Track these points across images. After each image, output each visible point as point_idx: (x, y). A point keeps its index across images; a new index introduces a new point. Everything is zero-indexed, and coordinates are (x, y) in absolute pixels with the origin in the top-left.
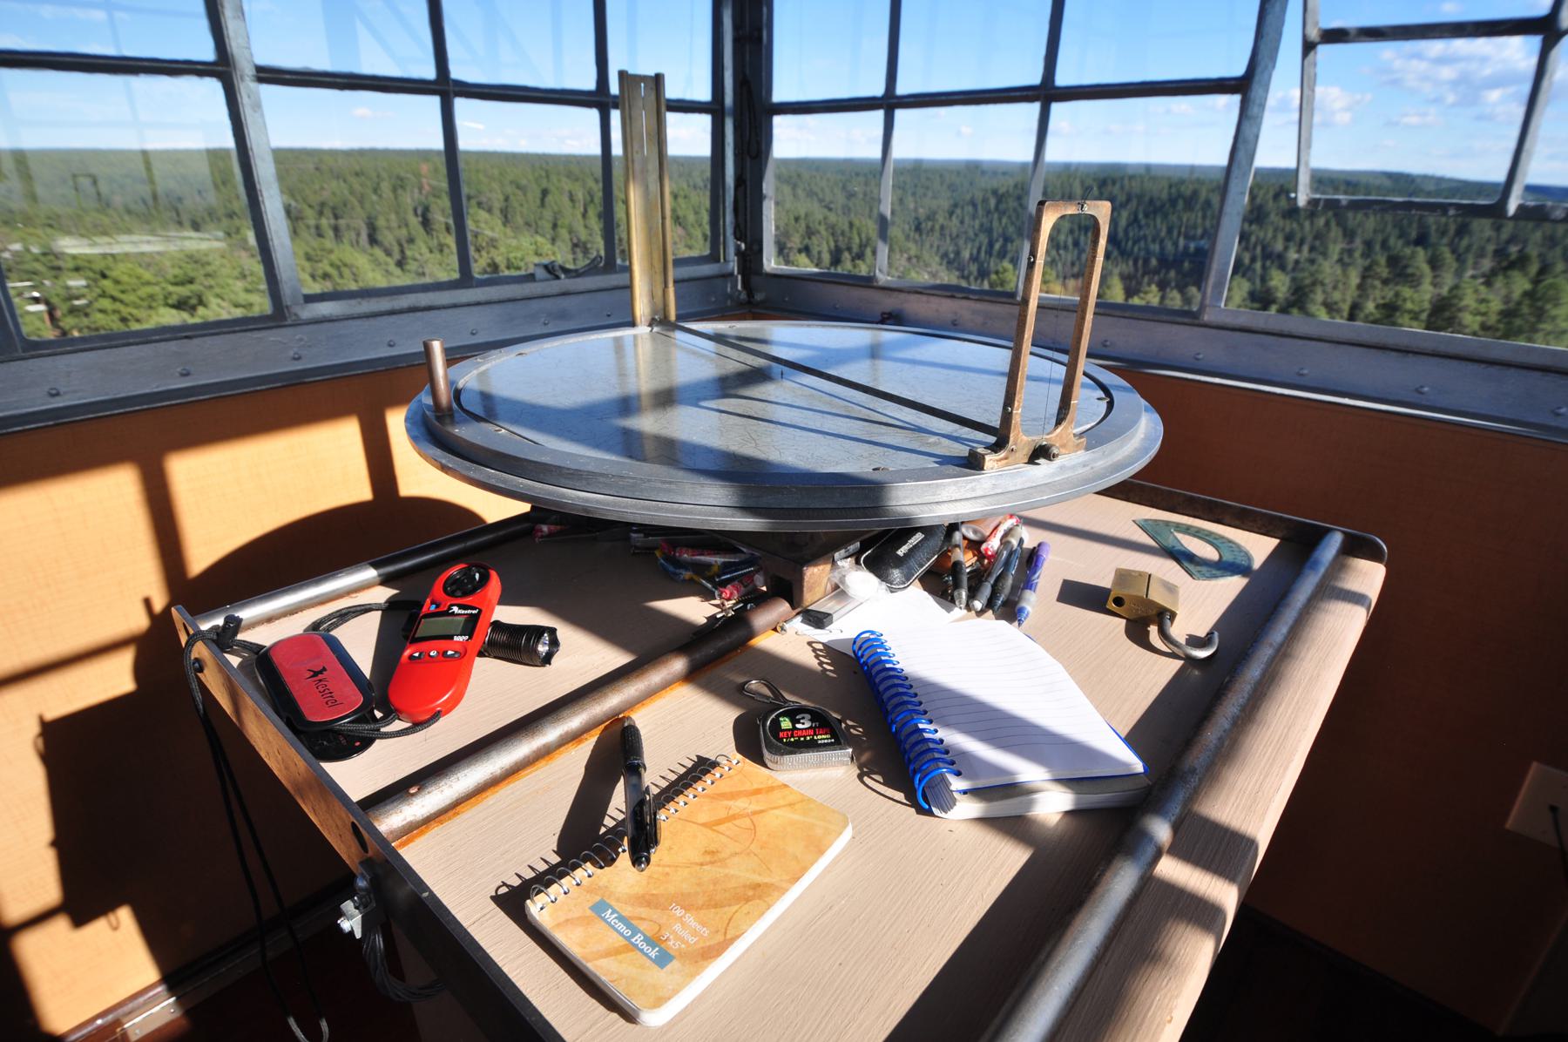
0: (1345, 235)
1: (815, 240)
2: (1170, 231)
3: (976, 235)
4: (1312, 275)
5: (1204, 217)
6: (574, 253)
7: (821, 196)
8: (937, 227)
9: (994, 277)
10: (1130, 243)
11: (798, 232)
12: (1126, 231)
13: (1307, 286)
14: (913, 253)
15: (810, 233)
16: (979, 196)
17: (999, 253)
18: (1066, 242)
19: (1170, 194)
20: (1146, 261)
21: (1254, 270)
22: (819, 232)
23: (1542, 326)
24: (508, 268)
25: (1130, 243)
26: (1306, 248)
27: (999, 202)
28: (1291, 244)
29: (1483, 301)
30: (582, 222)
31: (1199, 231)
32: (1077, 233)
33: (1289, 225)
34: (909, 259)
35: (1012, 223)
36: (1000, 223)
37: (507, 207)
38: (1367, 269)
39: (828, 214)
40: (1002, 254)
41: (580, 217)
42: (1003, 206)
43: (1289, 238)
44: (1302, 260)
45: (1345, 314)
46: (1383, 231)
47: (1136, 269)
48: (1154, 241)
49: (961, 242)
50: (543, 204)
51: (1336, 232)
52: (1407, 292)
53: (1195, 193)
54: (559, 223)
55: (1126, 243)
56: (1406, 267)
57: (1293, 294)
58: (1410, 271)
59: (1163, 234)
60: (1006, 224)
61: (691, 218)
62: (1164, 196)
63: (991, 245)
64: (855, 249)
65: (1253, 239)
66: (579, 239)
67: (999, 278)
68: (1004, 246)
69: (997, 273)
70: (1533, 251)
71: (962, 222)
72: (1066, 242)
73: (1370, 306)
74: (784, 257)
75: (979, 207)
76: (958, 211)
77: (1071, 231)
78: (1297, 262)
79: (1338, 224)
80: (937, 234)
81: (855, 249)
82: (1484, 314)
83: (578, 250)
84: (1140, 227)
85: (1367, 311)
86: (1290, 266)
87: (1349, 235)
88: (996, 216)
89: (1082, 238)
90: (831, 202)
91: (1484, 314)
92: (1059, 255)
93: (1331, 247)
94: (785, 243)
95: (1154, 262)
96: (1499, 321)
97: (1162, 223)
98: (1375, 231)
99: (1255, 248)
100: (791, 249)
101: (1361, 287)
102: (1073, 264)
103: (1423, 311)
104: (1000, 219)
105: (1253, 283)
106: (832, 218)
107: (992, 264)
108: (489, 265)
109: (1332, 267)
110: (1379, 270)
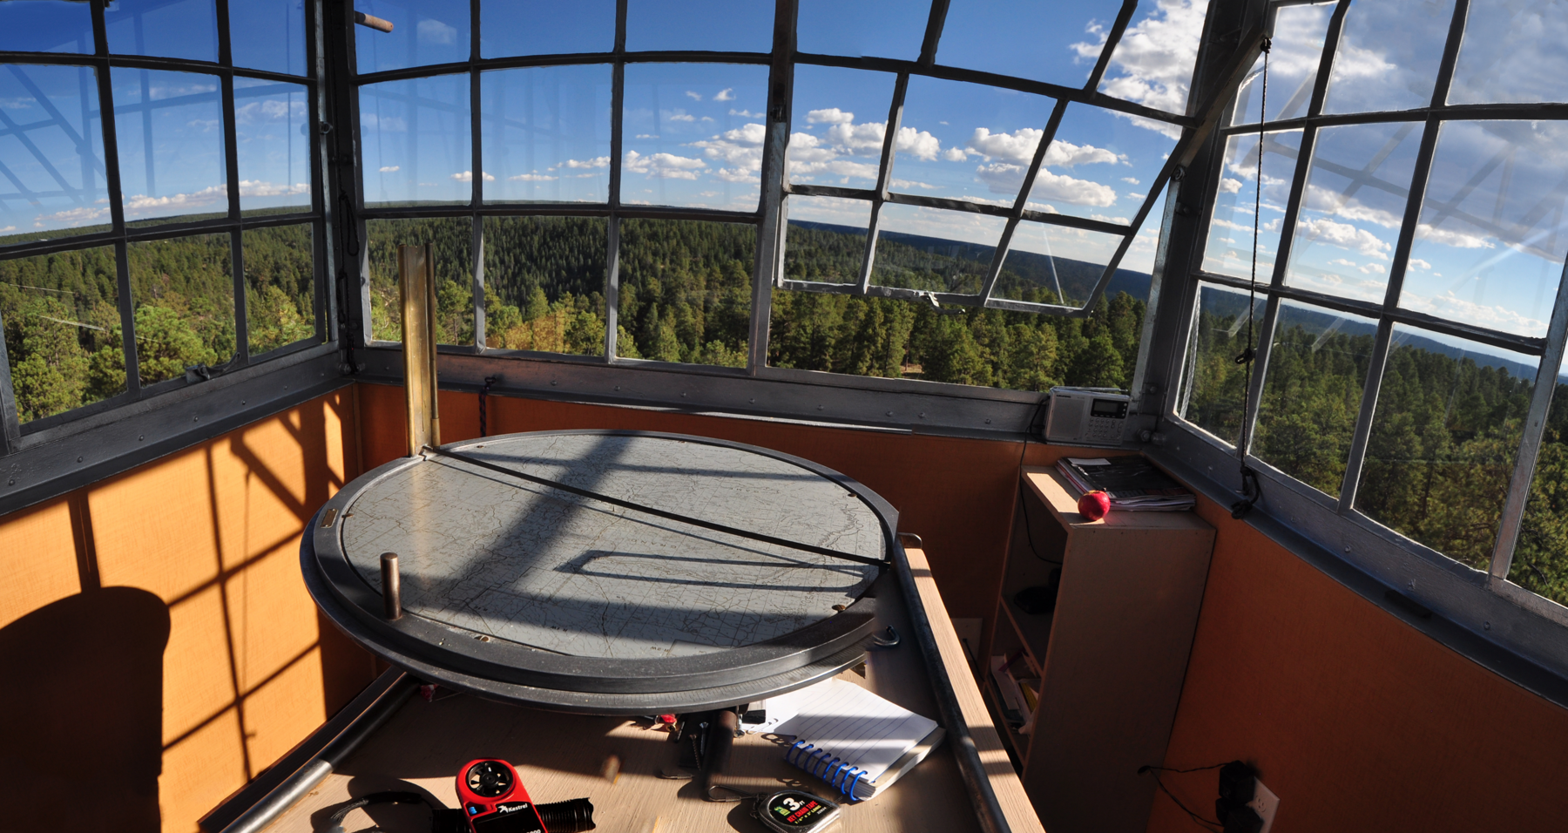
0: (691, 252)
1: (283, 273)
4: (676, 280)
5: (594, 240)
6: (77, 306)
7: (284, 237)
8: (387, 254)
9: (442, 292)
10: (544, 260)
11: (267, 268)
13: (673, 288)
15: (277, 268)
17: (441, 272)
18: (493, 261)
19: (567, 223)
20: (558, 274)
21: (636, 278)
22: (285, 266)
23: (815, 310)
24: (26, 325)
25: (544, 260)
26: (667, 261)
27: (435, 233)
28: (658, 258)
29: (781, 295)
30: (82, 280)
31: (593, 250)
32: (501, 254)
33: (654, 245)
35: (449, 248)
36: (439, 249)
37: (21, 276)
38: (710, 275)
39: (292, 250)
41: (80, 276)
43: (655, 254)
44: (667, 269)
45: (702, 307)
46: (714, 249)
47: (552, 280)
48: (561, 257)
50: (50, 270)
51: (684, 250)
52: (737, 291)
54: (63, 283)
55: (541, 261)
56: (732, 273)
57: (665, 294)
58: (735, 275)
59: (567, 253)
60: (444, 249)
61: (173, 265)
65: (631, 255)
66: (80, 294)
67: (446, 293)
68: (444, 266)
70: (802, 262)
72: (493, 261)
73: (716, 300)
74: (257, 290)
75: (420, 237)
77: (497, 253)
78: (664, 270)
79: (685, 244)
80: (387, 259)
82: (784, 304)
83: (80, 303)
84: (550, 248)
85: (715, 305)
86: (660, 274)
87: (694, 252)
89: (506, 258)
90: (292, 242)
91: (784, 304)
92: (490, 271)
93: (684, 260)
94: (257, 278)
96: (792, 308)
97: (565, 244)
98: (709, 249)
99: (633, 262)
100: (262, 282)
101: (707, 287)
102: (502, 278)
103: (749, 303)
104: (438, 246)
105: (637, 287)
106: (296, 253)
107: (437, 281)
108: (10, 325)
109: (687, 274)
110: (716, 276)
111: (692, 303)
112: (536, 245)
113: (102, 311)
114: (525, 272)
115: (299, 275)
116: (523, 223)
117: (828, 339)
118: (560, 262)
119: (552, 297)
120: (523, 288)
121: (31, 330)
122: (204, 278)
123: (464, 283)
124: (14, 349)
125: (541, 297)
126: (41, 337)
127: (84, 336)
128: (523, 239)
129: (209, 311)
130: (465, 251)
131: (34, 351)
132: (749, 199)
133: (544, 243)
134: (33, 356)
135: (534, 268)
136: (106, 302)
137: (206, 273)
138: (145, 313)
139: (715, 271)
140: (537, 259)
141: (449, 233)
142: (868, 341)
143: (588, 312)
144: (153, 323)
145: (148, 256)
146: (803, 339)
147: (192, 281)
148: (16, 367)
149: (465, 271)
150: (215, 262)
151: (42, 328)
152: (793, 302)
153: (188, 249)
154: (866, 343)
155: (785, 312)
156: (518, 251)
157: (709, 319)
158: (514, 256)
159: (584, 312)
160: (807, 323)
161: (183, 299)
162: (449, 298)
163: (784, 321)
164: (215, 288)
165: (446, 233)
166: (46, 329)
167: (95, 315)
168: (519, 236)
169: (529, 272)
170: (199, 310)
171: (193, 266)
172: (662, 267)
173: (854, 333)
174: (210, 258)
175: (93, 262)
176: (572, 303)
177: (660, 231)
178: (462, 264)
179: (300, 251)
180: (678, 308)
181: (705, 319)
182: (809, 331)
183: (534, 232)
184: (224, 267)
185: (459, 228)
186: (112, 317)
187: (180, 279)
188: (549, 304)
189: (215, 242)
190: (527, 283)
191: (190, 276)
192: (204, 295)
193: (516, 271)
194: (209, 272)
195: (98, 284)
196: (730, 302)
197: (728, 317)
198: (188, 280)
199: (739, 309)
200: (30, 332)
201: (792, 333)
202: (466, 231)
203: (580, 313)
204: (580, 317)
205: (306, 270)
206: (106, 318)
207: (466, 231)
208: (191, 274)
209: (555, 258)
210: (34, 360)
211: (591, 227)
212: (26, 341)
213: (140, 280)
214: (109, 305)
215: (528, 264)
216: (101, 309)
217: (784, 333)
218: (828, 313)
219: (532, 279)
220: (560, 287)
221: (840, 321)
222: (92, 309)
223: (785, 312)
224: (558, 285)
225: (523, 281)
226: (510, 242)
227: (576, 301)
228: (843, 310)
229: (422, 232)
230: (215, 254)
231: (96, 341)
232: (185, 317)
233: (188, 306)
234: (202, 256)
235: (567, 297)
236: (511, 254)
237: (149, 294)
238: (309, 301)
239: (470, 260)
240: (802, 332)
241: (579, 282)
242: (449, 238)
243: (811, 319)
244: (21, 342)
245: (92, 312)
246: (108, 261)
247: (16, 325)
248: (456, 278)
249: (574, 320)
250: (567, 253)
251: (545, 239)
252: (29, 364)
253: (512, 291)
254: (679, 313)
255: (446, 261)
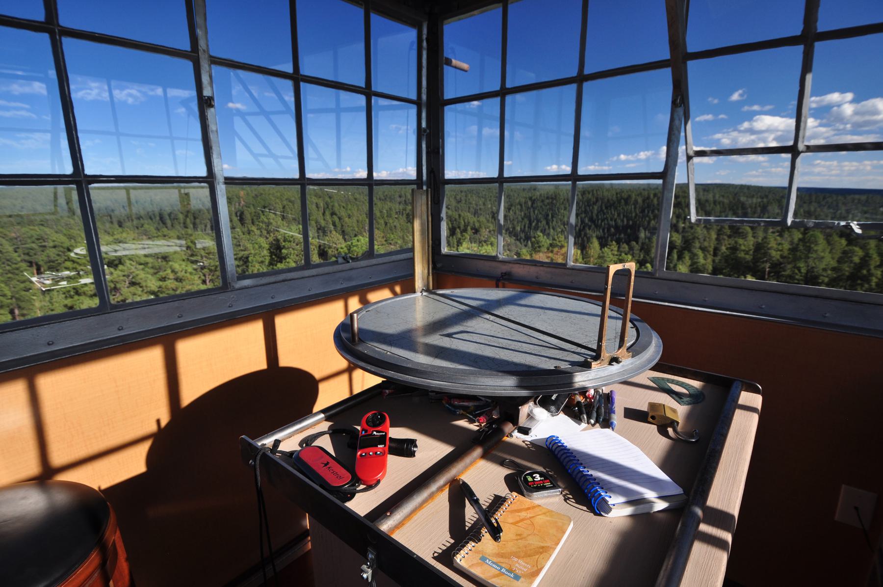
2: (619, 215)
3: (523, 219)
4: (692, 234)
5: (635, 208)
6: (318, 233)
9: (533, 239)
10: (600, 221)
12: (597, 215)
14: (491, 228)
16: (523, 200)
17: (535, 228)
19: (617, 198)
20: (609, 230)
23: (810, 255)
24: (284, 241)
25: (600, 221)
27: (533, 203)
28: (680, 220)
29: (779, 244)
30: (322, 218)
31: (634, 215)
34: (490, 232)
35: (540, 213)
38: (719, 230)
40: (536, 228)
41: (321, 215)
42: (535, 205)
44: (686, 227)
45: (712, 253)
47: (604, 234)
48: (611, 220)
49: (515, 223)
52: (741, 241)
53: (629, 197)
57: (684, 244)
58: (741, 230)
59: (616, 217)
60: (537, 213)
62: (614, 198)
63: (530, 224)
64: (462, 227)
66: (321, 226)
67: (536, 240)
68: (537, 224)
69: (535, 237)
71: (515, 213)
73: (724, 248)
76: (513, 208)
78: (684, 228)
81: (462, 227)
82: (781, 251)
83: (320, 231)
84: (604, 214)
85: (722, 251)
86: (681, 230)
88: (532, 210)
91: (781, 251)
92: (565, 228)
95: (612, 230)
96: (789, 254)
97: (615, 211)
101: (717, 239)
103: (750, 250)
104: (534, 212)
107: (532, 233)
108: (274, 240)
109: (702, 230)
110: (725, 231)
111: (703, 249)
112: (595, 212)
113: (333, 238)
114: (587, 229)
115: (450, 226)
116: (588, 198)
117: (822, 277)
118: (611, 222)
119: (603, 245)
120: (585, 238)
121: (287, 244)
122: (395, 224)
123: (548, 235)
124: (275, 255)
125: (596, 244)
126: (293, 249)
127: (321, 251)
128: (588, 208)
129: (397, 243)
130: (550, 215)
131: (288, 258)
132: (757, 174)
133: (601, 211)
134: (288, 260)
135: (593, 226)
136: (336, 232)
137: (397, 220)
138: (358, 241)
139: (725, 229)
140: (595, 221)
141: (541, 204)
142: (862, 280)
143: (626, 254)
144: (362, 247)
145: (364, 207)
146: (797, 277)
147: (388, 224)
148: (276, 266)
149: (549, 227)
150: (403, 214)
151: (295, 244)
152: (789, 249)
153: (387, 205)
154: (859, 282)
155: (782, 257)
156: (583, 215)
157: (717, 261)
158: (581, 218)
159: (623, 254)
160: (802, 265)
161: (382, 235)
162: (538, 243)
163: (781, 264)
164: (402, 230)
165: (539, 204)
166: (297, 245)
167: (329, 240)
168: (585, 206)
169: (589, 229)
170: (391, 242)
171: (389, 216)
172: (683, 225)
173: (847, 274)
174: (400, 212)
175: (330, 207)
176: (616, 249)
177: (683, 201)
178: (548, 223)
179: (452, 211)
180: (692, 253)
181: (714, 261)
182: (803, 270)
183: (595, 203)
184: (407, 218)
185: (548, 201)
186: (339, 242)
187: (381, 223)
188: (601, 249)
189: (403, 202)
190: (588, 236)
191: (387, 221)
192: (395, 233)
193: (582, 228)
194: (399, 220)
195: (332, 221)
196: (734, 249)
197: (732, 259)
198: (386, 224)
199: (742, 255)
200: (286, 246)
201: (788, 272)
202: (552, 203)
203: (620, 255)
204: (620, 258)
205: (455, 222)
206: (335, 241)
207: (552, 203)
208: (388, 220)
209: (607, 220)
210: (288, 263)
211: (633, 199)
212: (284, 251)
213: (358, 221)
214: (337, 234)
215: (590, 224)
216: (332, 236)
217: (780, 272)
218: (823, 258)
219: (591, 233)
220: (609, 239)
221: (834, 264)
222: (327, 236)
223: (782, 257)
224: (608, 237)
225: (585, 235)
226: (579, 210)
227: (619, 248)
228: (838, 255)
229: (525, 203)
230: (403, 210)
231: (329, 255)
232: (382, 245)
233: (385, 239)
234: (395, 210)
235: (613, 245)
236: (579, 218)
237: (363, 230)
238: (455, 241)
239: (553, 221)
240: (796, 271)
241: (622, 236)
242: (541, 207)
243: (806, 262)
244: (280, 251)
245: (327, 238)
246: (339, 208)
247: (277, 240)
248: (543, 231)
249: (616, 260)
250: (616, 217)
251: (601, 208)
252: (284, 265)
253: (578, 241)
254: (693, 256)
255: (538, 221)
